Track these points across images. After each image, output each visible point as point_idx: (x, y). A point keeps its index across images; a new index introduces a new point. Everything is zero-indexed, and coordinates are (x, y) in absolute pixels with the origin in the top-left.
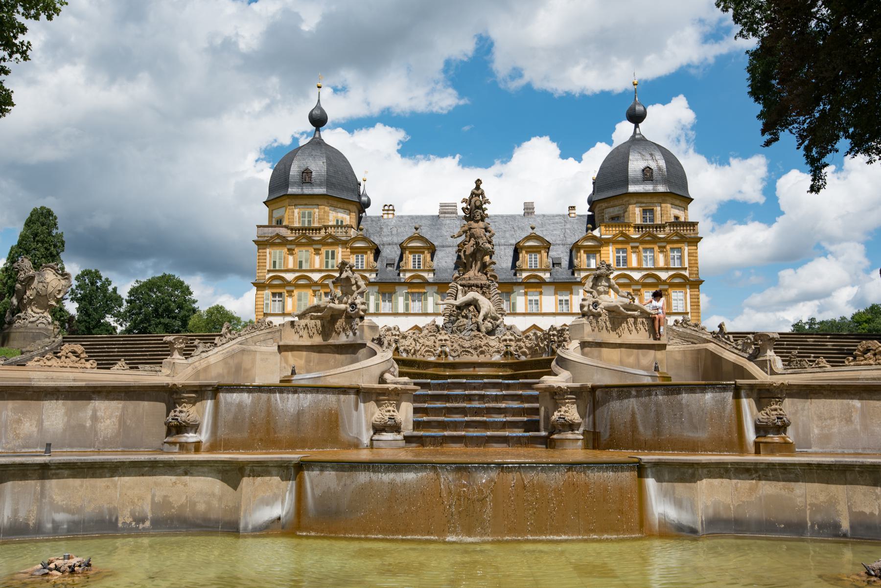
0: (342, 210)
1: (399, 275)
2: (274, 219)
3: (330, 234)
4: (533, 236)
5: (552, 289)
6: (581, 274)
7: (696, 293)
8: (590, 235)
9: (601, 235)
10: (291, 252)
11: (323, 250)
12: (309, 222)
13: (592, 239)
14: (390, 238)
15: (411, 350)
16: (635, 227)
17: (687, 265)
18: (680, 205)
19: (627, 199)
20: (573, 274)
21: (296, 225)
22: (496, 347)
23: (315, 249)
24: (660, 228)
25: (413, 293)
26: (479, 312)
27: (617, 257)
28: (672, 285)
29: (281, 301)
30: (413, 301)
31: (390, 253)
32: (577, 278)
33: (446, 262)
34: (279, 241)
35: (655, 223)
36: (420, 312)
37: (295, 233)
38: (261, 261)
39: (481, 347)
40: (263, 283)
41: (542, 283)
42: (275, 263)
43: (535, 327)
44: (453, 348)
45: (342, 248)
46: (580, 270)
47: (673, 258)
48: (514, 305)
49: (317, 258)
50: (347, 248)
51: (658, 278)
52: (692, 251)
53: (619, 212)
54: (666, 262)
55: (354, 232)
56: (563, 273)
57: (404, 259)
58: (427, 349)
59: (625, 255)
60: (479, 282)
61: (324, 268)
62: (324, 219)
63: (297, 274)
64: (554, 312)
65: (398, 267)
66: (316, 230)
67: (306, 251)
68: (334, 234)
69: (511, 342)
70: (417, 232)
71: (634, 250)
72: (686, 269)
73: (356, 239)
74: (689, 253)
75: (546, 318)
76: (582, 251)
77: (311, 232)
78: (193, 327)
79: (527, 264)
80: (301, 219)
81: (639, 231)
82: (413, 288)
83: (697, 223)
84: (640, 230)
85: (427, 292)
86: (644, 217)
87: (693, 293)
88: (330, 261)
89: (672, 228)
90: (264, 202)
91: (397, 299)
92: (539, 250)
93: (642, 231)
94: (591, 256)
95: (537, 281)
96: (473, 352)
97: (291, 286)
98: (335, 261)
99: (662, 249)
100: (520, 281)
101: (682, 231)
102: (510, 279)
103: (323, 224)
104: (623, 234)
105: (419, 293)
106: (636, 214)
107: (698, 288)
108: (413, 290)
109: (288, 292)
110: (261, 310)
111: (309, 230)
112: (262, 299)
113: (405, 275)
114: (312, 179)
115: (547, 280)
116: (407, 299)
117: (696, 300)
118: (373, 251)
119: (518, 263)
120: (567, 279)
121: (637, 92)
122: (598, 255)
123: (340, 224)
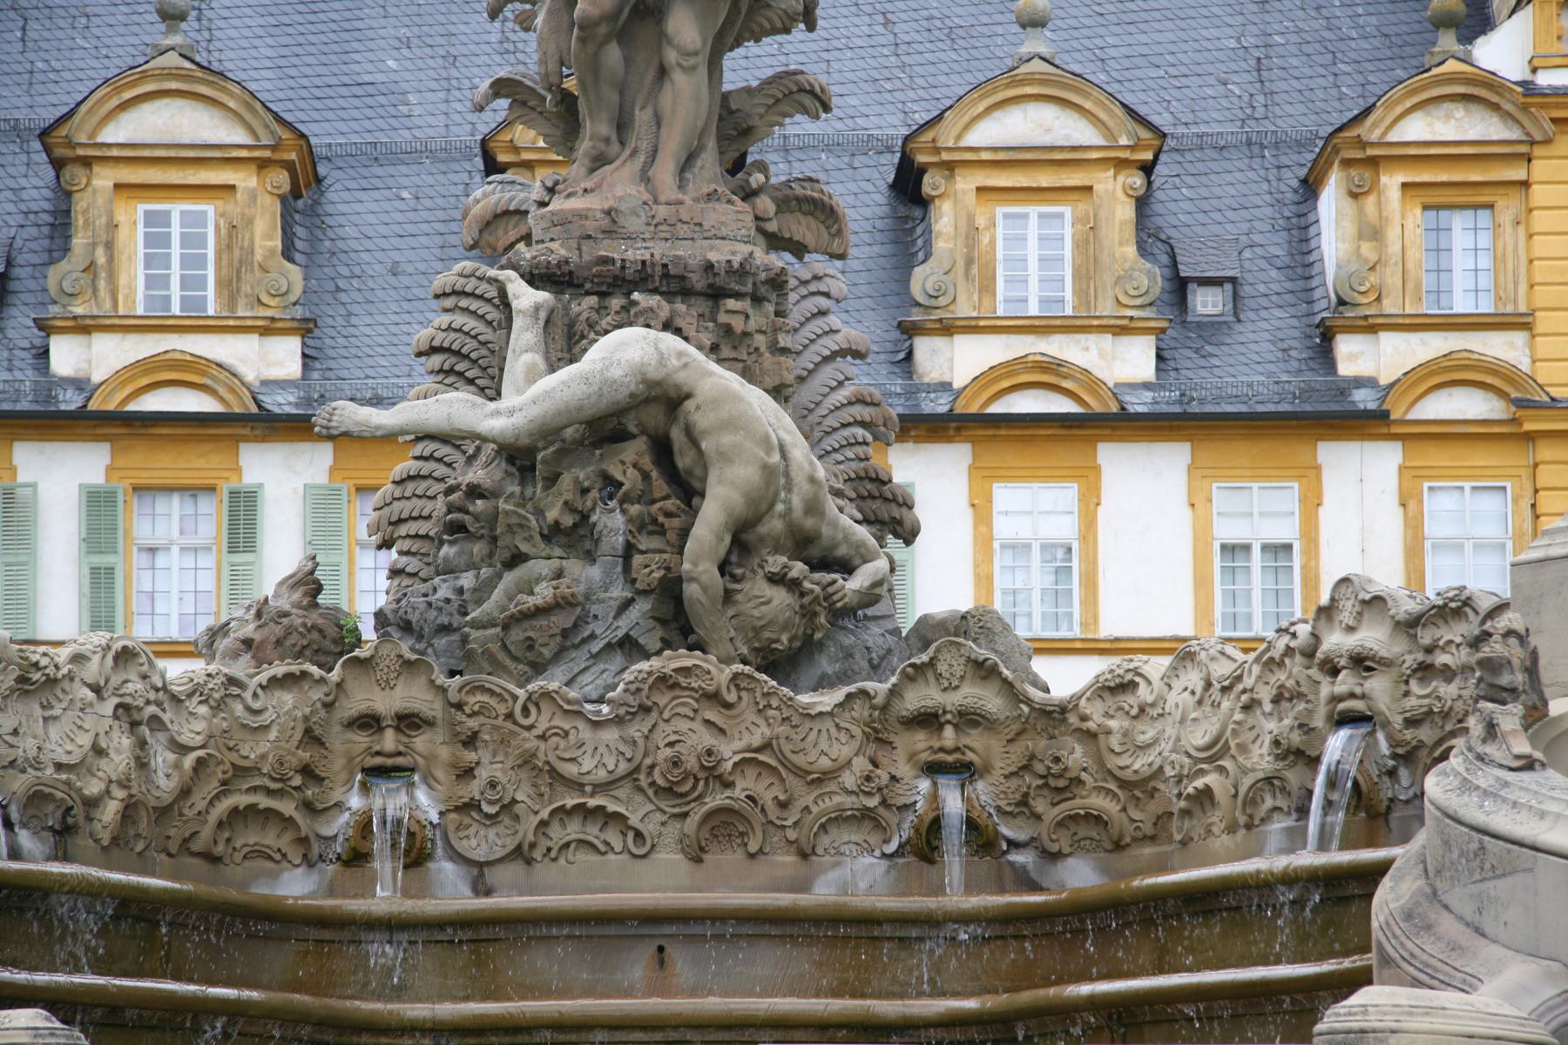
8: (1452, 66)
15: (92, 803)
22: (849, 780)
26: (689, 492)
39: (713, 775)
44: (474, 789)
46: (1370, 327)
57: (79, 241)
58: (242, 800)
60: (689, 253)
69: (975, 740)
70: (176, 40)
79: (988, 287)
96: (649, 828)
100: (941, 405)
115: (1139, 404)
119: (922, 279)
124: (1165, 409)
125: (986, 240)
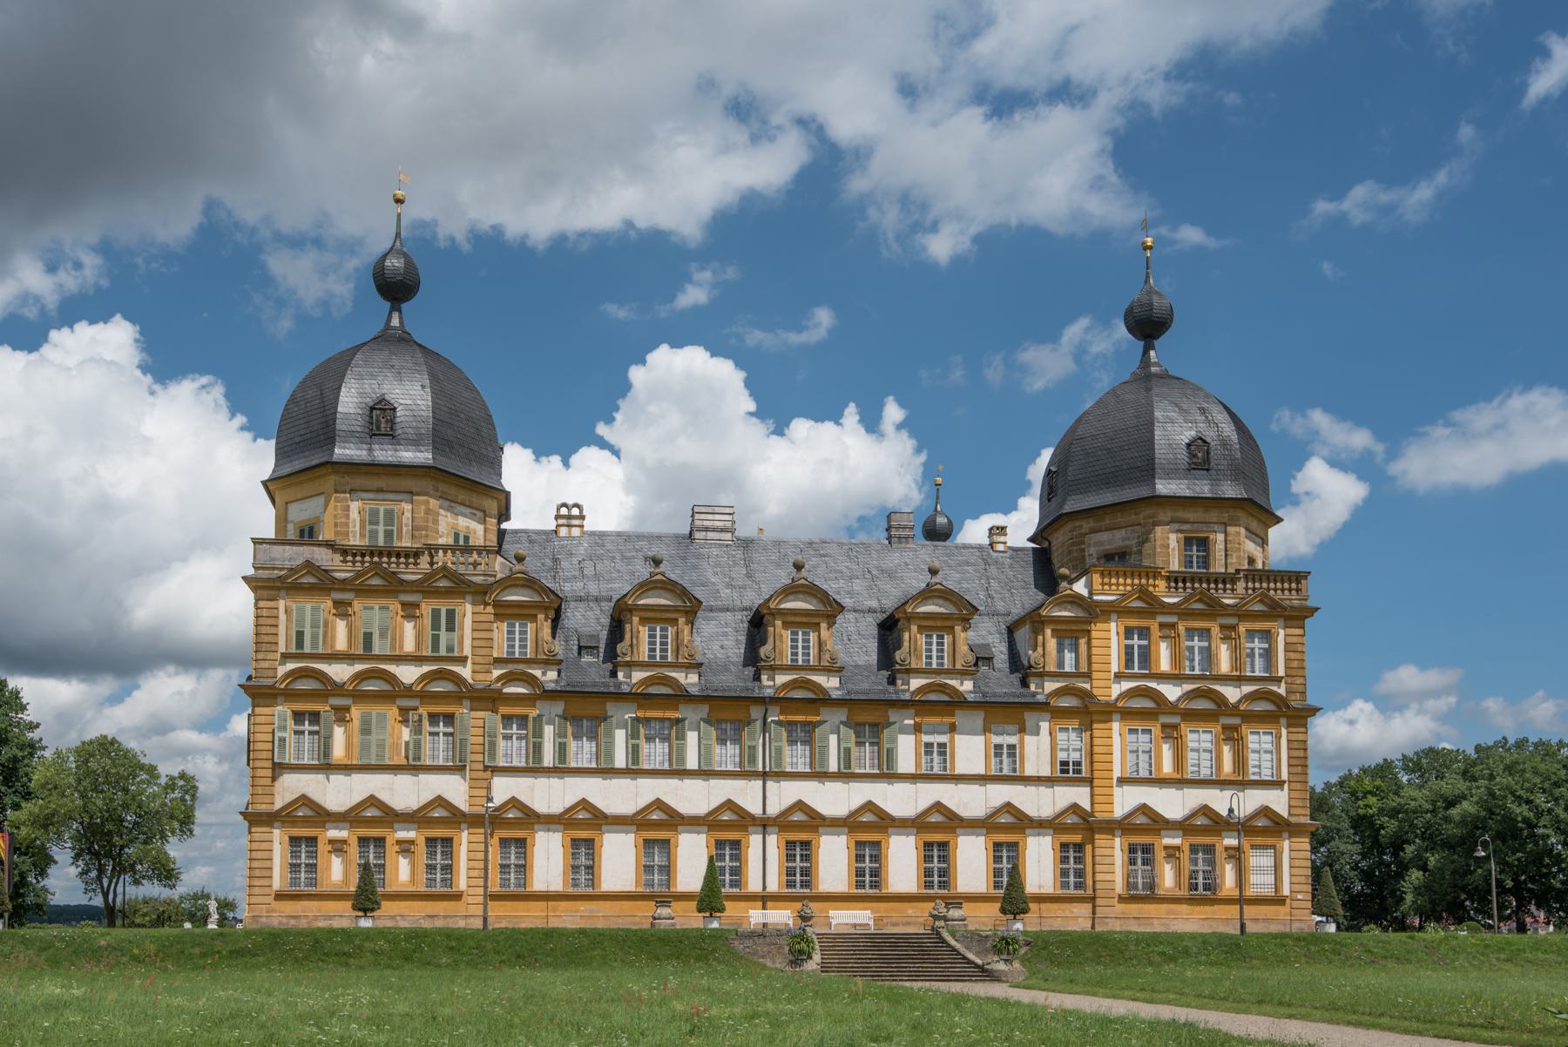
0: (467, 511)
1: (614, 674)
2: (290, 527)
3: (444, 568)
4: (936, 590)
5: (978, 718)
6: (1046, 684)
7: (1301, 737)
8: (1069, 592)
9: (1091, 593)
10: (342, 609)
11: (426, 608)
12: (389, 534)
13: (1071, 602)
14: (580, 585)
16: (1168, 579)
17: (1281, 673)
18: (1259, 531)
19: (1148, 512)
20: (1024, 683)
21: (355, 540)
23: (404, 605)
24: (1224, 582)
25: (648, 720)
27: (1126, 646)
28: (1251, 718)
29: (317, 733)
30: (649, 739)
31: (587, 620)
32: (1034, 695)
33: (722, 647)
34: (312, 580)
35: (1211, 570)
36: (666, 766)
37: (354, 562)
38: (264, 630)
40: (272, 687)
41: (956, 703)
42: (300, 635)
43: (938, 807)
45: (474, 604)
46: (1043, 675)
47: (1251, 655)
48: (891, 754)
49: (409, 628)
50: (486, 604)
51: (1220, 700)
52: (1294, 640)
53: (1127, 543)
54: (1236, 662)
55: (502, 563)
56: (1001, 682)
57: (628, 636)
59: (1145, 642)
61: (430, 654)
62: (426, 529)
63: (359, 667)
64: (983, 772)
65: (611, 655)
66: (407, 556)
67: (380, 608)
68: (454, 567)
71: (1166, 632)
72: (1278, 680)
73: (509, 582)
74: (1286, 643)
75: (962, 787)
76: (1048, 632)
77: (394, 559)
78: (43, 786)
80: (368, 527)
81: (1176, 588)
82: (651, 708)
83: (1305, 575)
84: (1180, 585)
85: (683, 720)
86: (1186, 556)
87: (1294, 737)
88: (443, 635)
89: (1250, 585)
90: (265, 483)
91: (611, 736)
92: (949, 624)
93: (1185, 588)
94: (1067, 642)
95: (946, 698)
97: (343, 695)
98: (456, 635)
99: (1229, 633)
100: (907, 696)
101: (1272, 592)
102: (885, 692)
103: (423, 541)
104: (1144, 594)
105: (662, 720)
106: (1169, 547)
107: (1305, 726)
108: (650, 714)
109: (336, 709)
110: (265, 755)
111: (389, 555)
112: (269, 728)
113: (630, 677)
114: (398, 426)
115: (971, 698)
116: (634, 735)
117: (1301, 753)
118: (552, 614)
119: (899, 655)
120: (1014, 695)
121: (1151, 265)
122: (1083, 642)
123: (461, 543)
124: (978, 700)
125: (919, 643)
